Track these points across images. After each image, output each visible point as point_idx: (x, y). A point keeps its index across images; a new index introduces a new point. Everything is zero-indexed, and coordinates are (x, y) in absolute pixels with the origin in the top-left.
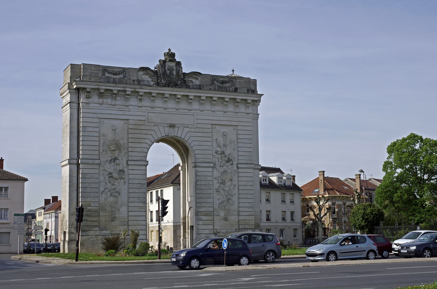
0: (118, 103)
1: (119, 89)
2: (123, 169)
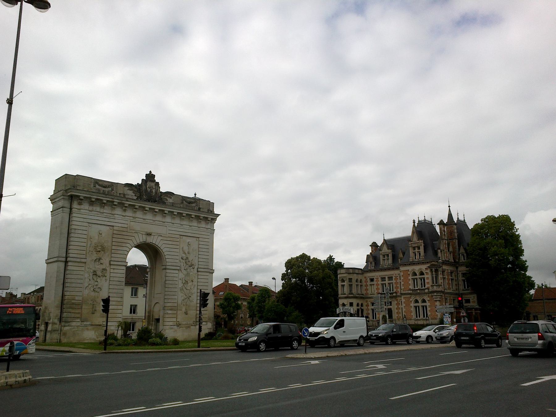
0: (105, 211)
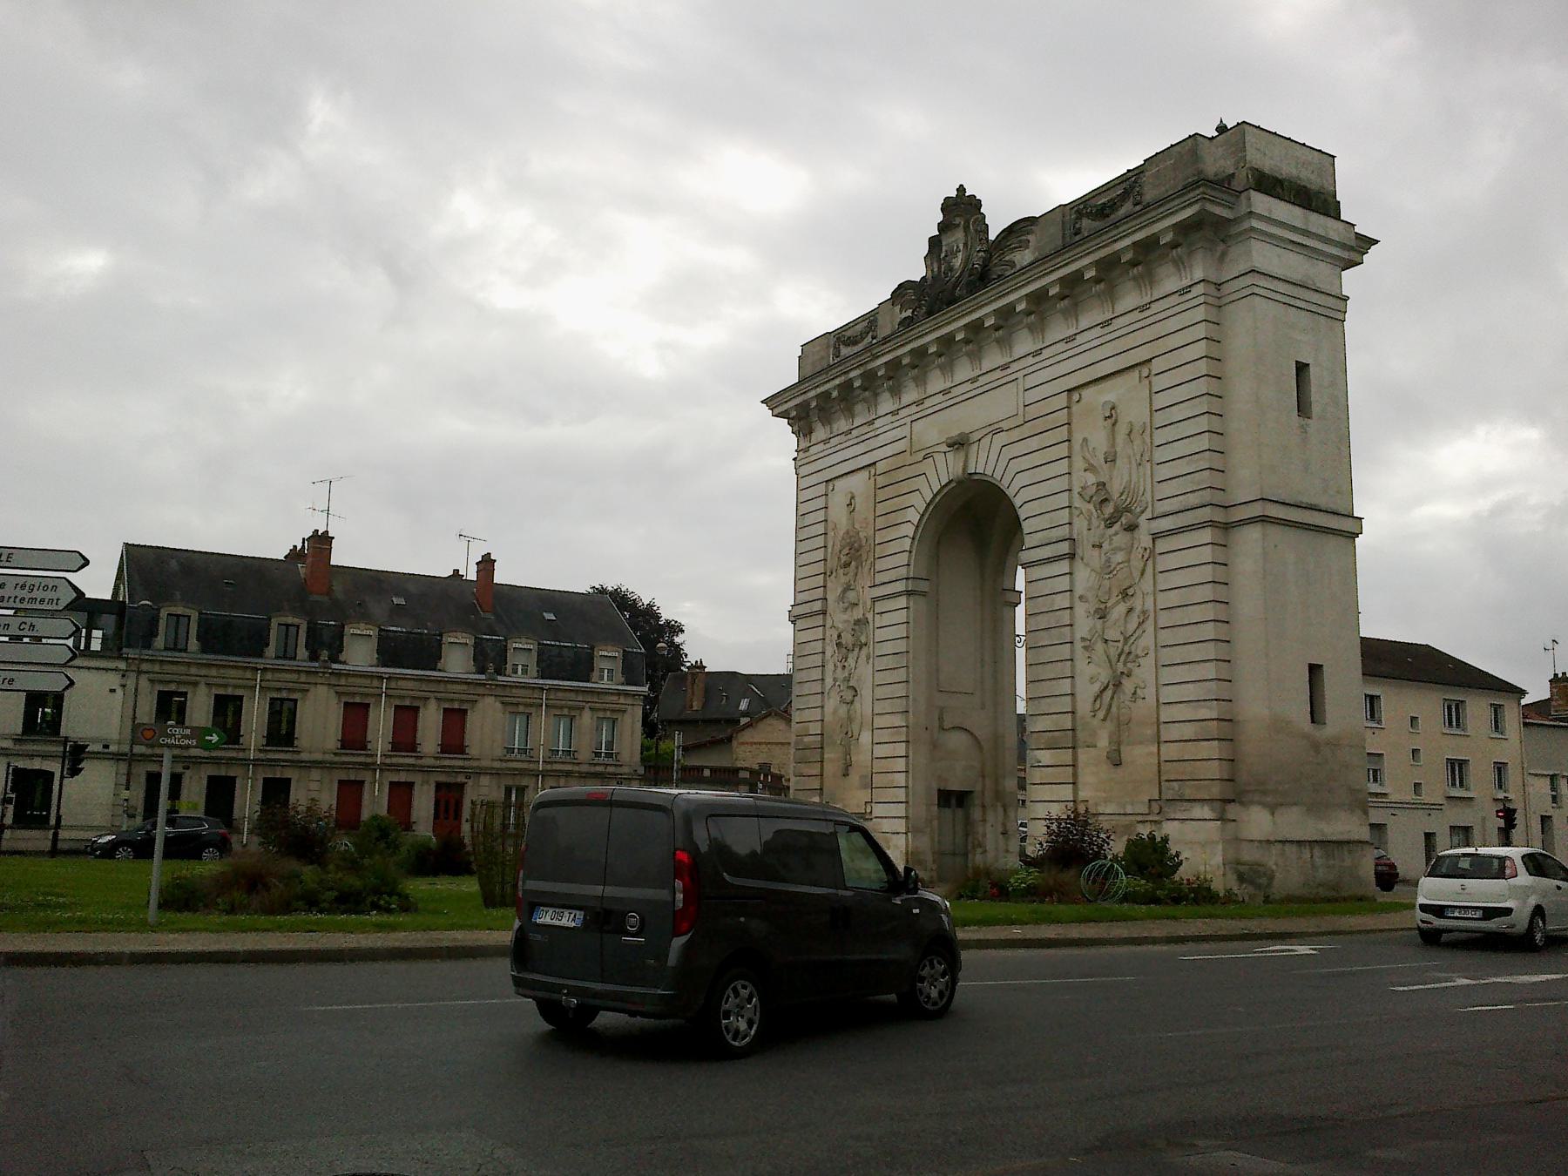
1: (837, 382)
2: (863, 615)
